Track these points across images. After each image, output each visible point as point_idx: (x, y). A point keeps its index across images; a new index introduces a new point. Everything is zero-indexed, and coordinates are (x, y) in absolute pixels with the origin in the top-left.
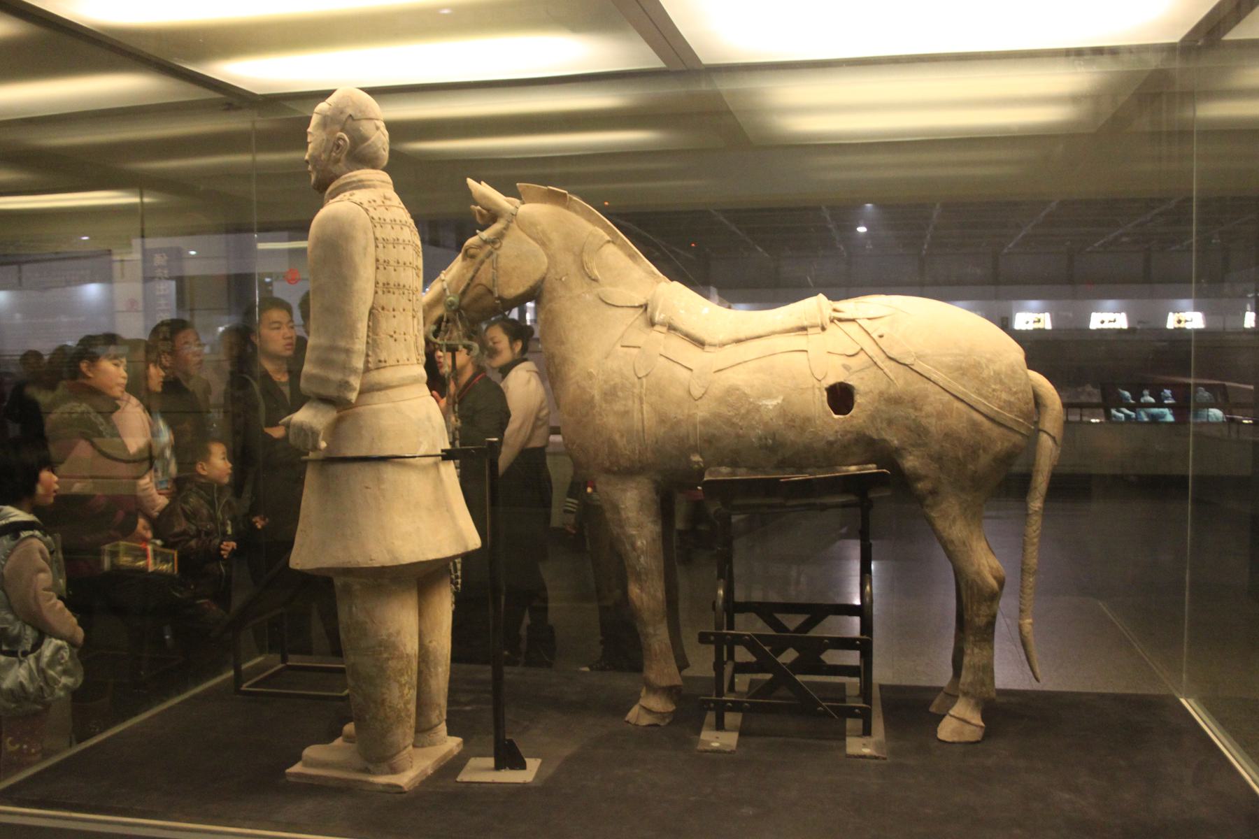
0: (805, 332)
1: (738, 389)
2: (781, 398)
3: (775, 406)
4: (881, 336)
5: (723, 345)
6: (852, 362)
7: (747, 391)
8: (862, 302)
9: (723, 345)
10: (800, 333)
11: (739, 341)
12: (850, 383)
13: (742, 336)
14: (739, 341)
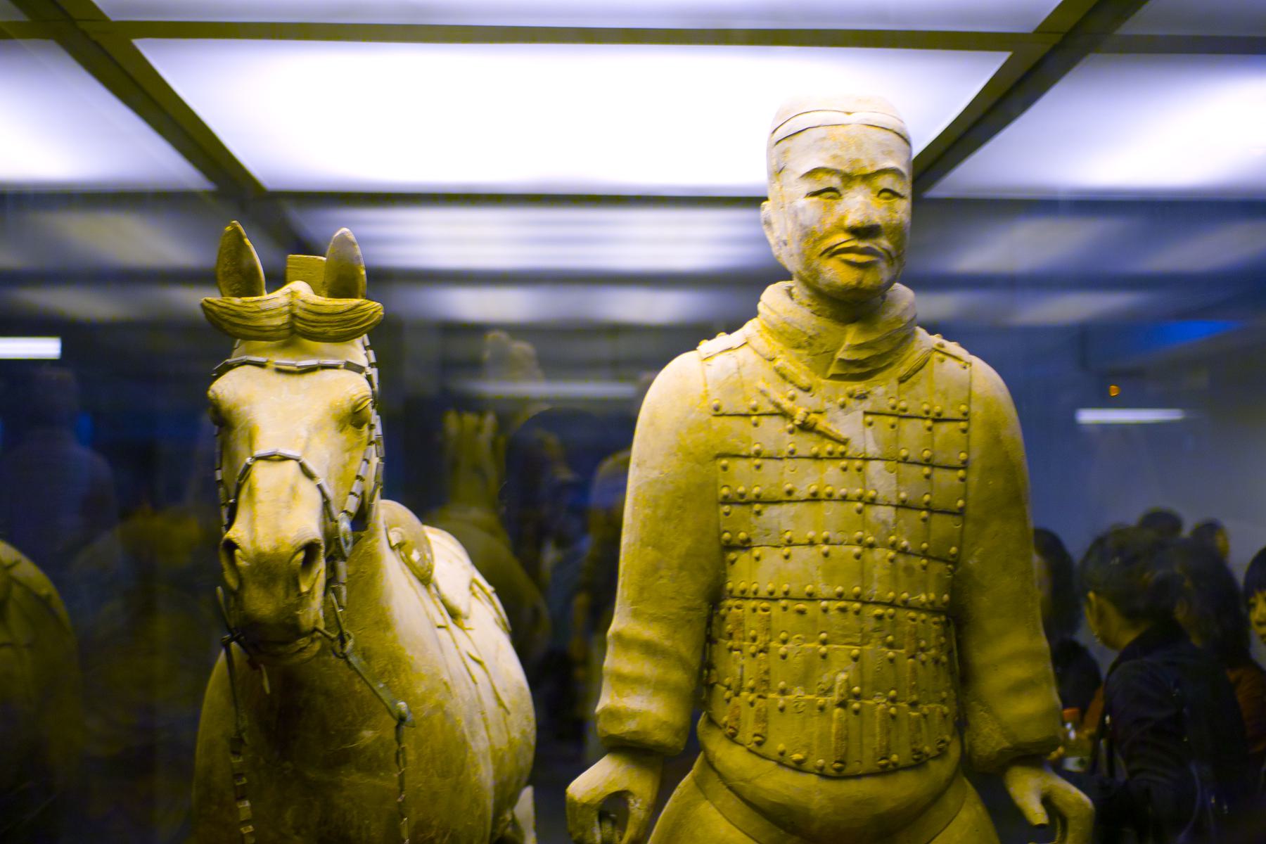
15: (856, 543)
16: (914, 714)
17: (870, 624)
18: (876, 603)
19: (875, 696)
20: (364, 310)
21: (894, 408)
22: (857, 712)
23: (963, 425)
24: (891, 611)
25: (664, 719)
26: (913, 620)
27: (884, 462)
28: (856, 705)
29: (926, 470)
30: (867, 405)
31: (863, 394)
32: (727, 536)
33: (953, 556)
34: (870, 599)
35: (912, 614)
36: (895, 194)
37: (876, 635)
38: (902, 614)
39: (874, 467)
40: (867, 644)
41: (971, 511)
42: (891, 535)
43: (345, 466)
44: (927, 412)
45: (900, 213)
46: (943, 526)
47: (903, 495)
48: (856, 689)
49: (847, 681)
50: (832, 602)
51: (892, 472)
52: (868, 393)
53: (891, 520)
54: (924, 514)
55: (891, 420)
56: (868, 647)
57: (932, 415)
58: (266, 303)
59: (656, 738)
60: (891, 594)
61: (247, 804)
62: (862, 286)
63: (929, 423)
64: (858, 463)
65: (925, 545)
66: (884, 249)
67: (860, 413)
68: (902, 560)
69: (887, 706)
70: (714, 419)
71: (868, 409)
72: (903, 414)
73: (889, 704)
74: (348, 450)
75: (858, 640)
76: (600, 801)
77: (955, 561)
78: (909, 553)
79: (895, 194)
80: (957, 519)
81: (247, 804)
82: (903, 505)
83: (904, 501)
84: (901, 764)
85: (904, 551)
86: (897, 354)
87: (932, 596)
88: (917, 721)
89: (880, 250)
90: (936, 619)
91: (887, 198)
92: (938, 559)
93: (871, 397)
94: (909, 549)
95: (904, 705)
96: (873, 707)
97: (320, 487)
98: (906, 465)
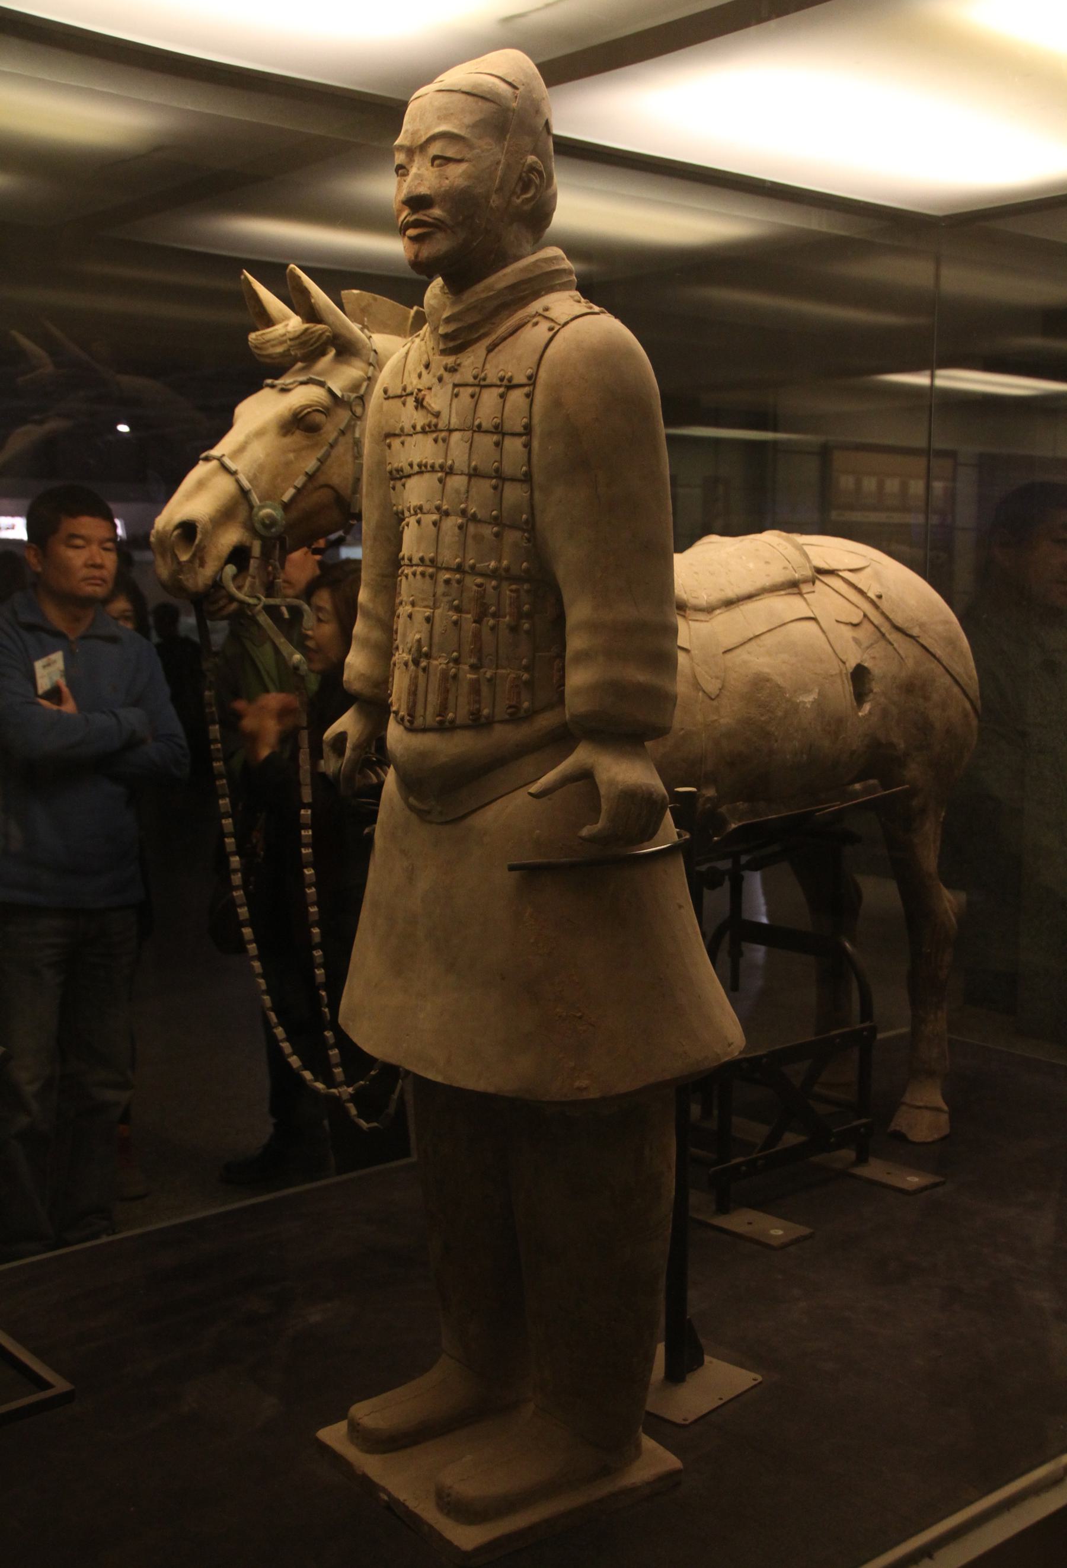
0: (795, 590)
1: (768, 680)
2: (817, 690)
3: (813, 702)
4: (880, 597)
5: (709, 610)
6: (860, 634)
7: (780, 681)
8: (711, 543)
9: (709, 610)
10: (790, 591)
11: (729, 603)
12: (866, 665)
13: (731, 593)
14: (729, 603)
15: (460, 514)
16: (469, 676)
17: (441, 588)
18: (448, 569)
19: (440, 657)
20: (312, 333)
21: (475, 377)
22: (424, 669)
23: (526, 389)
24: (458, 576)
25: (363, 672)
26: (480, 586)
27: (462, 433)
28: (424, 664)
29: (495, 438)
30: (457, 378)
31: (453, 367)
32: (395, 508)
33: (527, 522)
34: (442, 565)
35: (479, 580)
36: (448, 160)
37: (446, 599)
38: (472, 581)
39: (456, 437)
40: (438, 608)
41: (538, 477)
42: (462, 504)
43: (288, 464)
44: (502, 379)
45: (450, 179)
46: (514, 494)
47: (473, 464)
48: (425, 649)
49: (419, 641)
50: (420, 567)
51: (466, 442)
52: (459, 365)
53: (463, 489)
54: (494, 481)
55: (470, 390)
56: (438, 612)
57: (505, 382)
58: (268, 335)
59: (355, 688)
60: (458, 560)
61: (217, 727)
62: (420, 259)
63: (501, 390)
64: (443, 434)
65: (494, 513)
66: (435, 219)
67: (450, 386)
68: (472, 529)
69: (447, 667)
70: (386, 403)
71: (456, 382)
72: (482, 383)
73: (451, 665)
74: (294, 451)
75: (431, 604)
76: (331, 739)
77: (531, 527)
78: (480, 521)
79: (448, 160)
80: (526, 487)
81: (217, 727)
82: (474, 474)
83: (475, 469)
84: (458, 722)
85: (474, 518)
86: (494, 324)
87: (505, 563)
88: (477, 681)
89: (430, 220)
90: (514, 587)
91: (440, 166)
92: (513, 527)
93: (462, 370)
94: (479, 516)
95: (466, 667)
96: (437, 666)
97: (238, 481)
98: (482, 434)
